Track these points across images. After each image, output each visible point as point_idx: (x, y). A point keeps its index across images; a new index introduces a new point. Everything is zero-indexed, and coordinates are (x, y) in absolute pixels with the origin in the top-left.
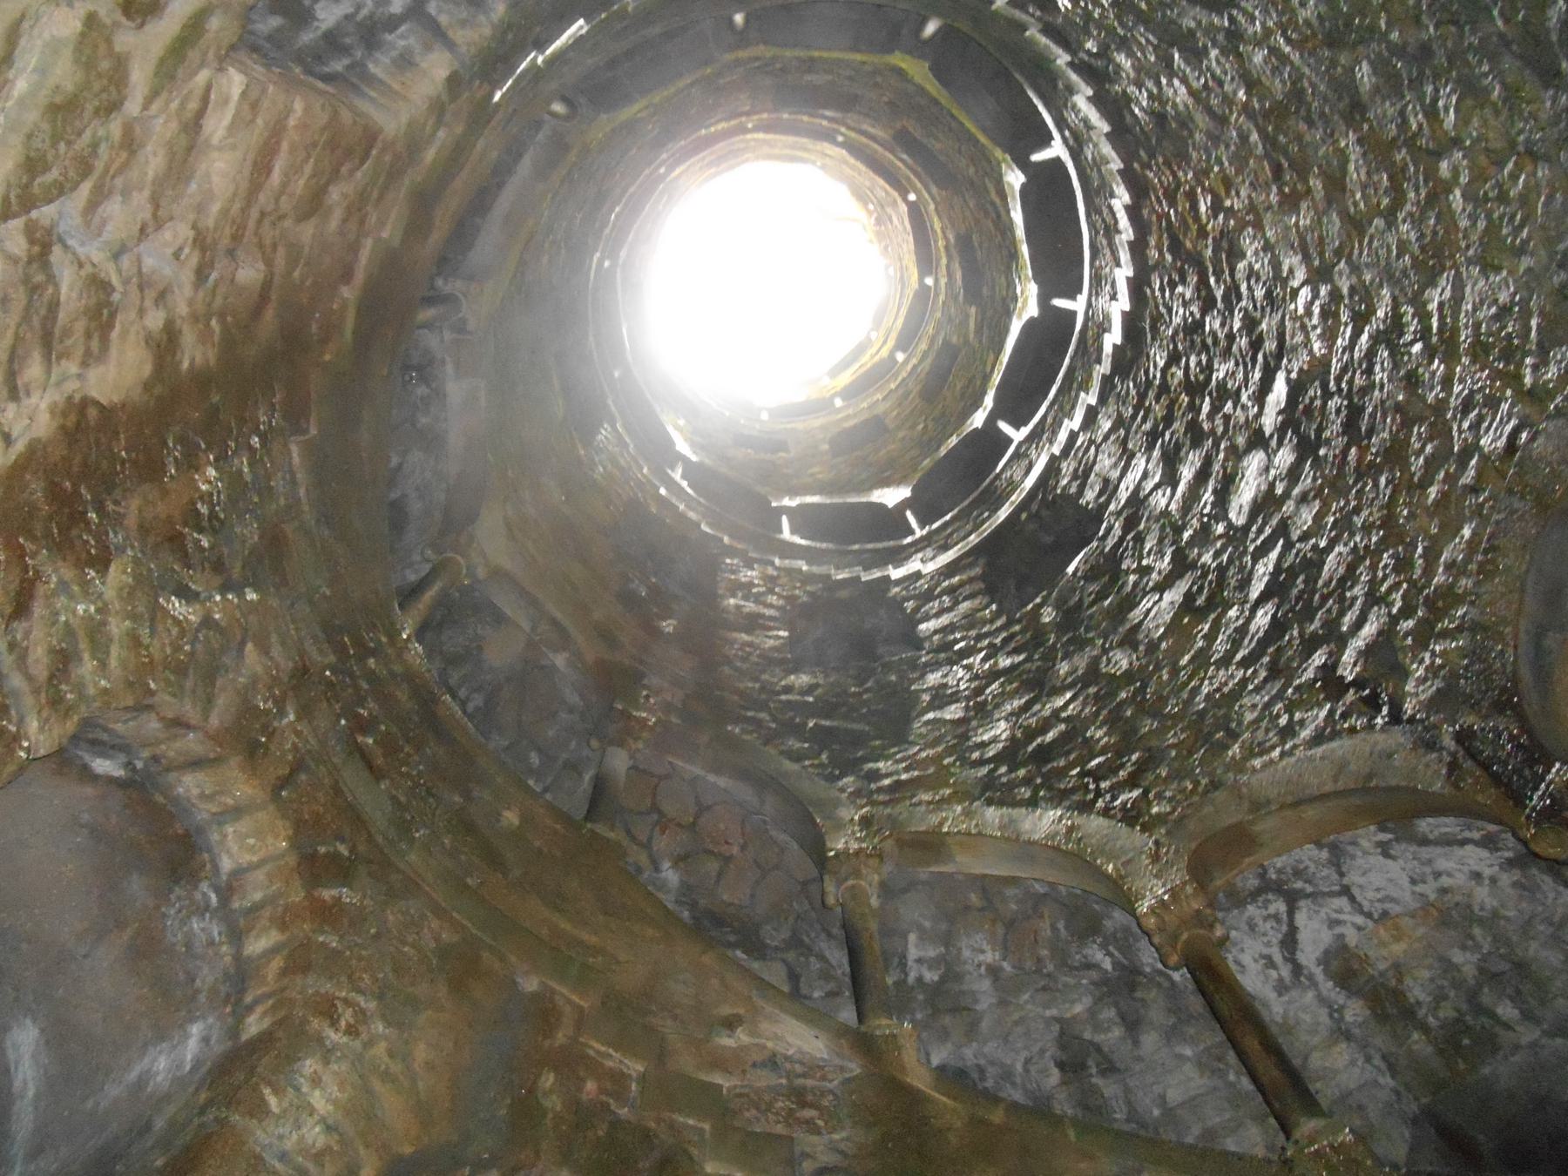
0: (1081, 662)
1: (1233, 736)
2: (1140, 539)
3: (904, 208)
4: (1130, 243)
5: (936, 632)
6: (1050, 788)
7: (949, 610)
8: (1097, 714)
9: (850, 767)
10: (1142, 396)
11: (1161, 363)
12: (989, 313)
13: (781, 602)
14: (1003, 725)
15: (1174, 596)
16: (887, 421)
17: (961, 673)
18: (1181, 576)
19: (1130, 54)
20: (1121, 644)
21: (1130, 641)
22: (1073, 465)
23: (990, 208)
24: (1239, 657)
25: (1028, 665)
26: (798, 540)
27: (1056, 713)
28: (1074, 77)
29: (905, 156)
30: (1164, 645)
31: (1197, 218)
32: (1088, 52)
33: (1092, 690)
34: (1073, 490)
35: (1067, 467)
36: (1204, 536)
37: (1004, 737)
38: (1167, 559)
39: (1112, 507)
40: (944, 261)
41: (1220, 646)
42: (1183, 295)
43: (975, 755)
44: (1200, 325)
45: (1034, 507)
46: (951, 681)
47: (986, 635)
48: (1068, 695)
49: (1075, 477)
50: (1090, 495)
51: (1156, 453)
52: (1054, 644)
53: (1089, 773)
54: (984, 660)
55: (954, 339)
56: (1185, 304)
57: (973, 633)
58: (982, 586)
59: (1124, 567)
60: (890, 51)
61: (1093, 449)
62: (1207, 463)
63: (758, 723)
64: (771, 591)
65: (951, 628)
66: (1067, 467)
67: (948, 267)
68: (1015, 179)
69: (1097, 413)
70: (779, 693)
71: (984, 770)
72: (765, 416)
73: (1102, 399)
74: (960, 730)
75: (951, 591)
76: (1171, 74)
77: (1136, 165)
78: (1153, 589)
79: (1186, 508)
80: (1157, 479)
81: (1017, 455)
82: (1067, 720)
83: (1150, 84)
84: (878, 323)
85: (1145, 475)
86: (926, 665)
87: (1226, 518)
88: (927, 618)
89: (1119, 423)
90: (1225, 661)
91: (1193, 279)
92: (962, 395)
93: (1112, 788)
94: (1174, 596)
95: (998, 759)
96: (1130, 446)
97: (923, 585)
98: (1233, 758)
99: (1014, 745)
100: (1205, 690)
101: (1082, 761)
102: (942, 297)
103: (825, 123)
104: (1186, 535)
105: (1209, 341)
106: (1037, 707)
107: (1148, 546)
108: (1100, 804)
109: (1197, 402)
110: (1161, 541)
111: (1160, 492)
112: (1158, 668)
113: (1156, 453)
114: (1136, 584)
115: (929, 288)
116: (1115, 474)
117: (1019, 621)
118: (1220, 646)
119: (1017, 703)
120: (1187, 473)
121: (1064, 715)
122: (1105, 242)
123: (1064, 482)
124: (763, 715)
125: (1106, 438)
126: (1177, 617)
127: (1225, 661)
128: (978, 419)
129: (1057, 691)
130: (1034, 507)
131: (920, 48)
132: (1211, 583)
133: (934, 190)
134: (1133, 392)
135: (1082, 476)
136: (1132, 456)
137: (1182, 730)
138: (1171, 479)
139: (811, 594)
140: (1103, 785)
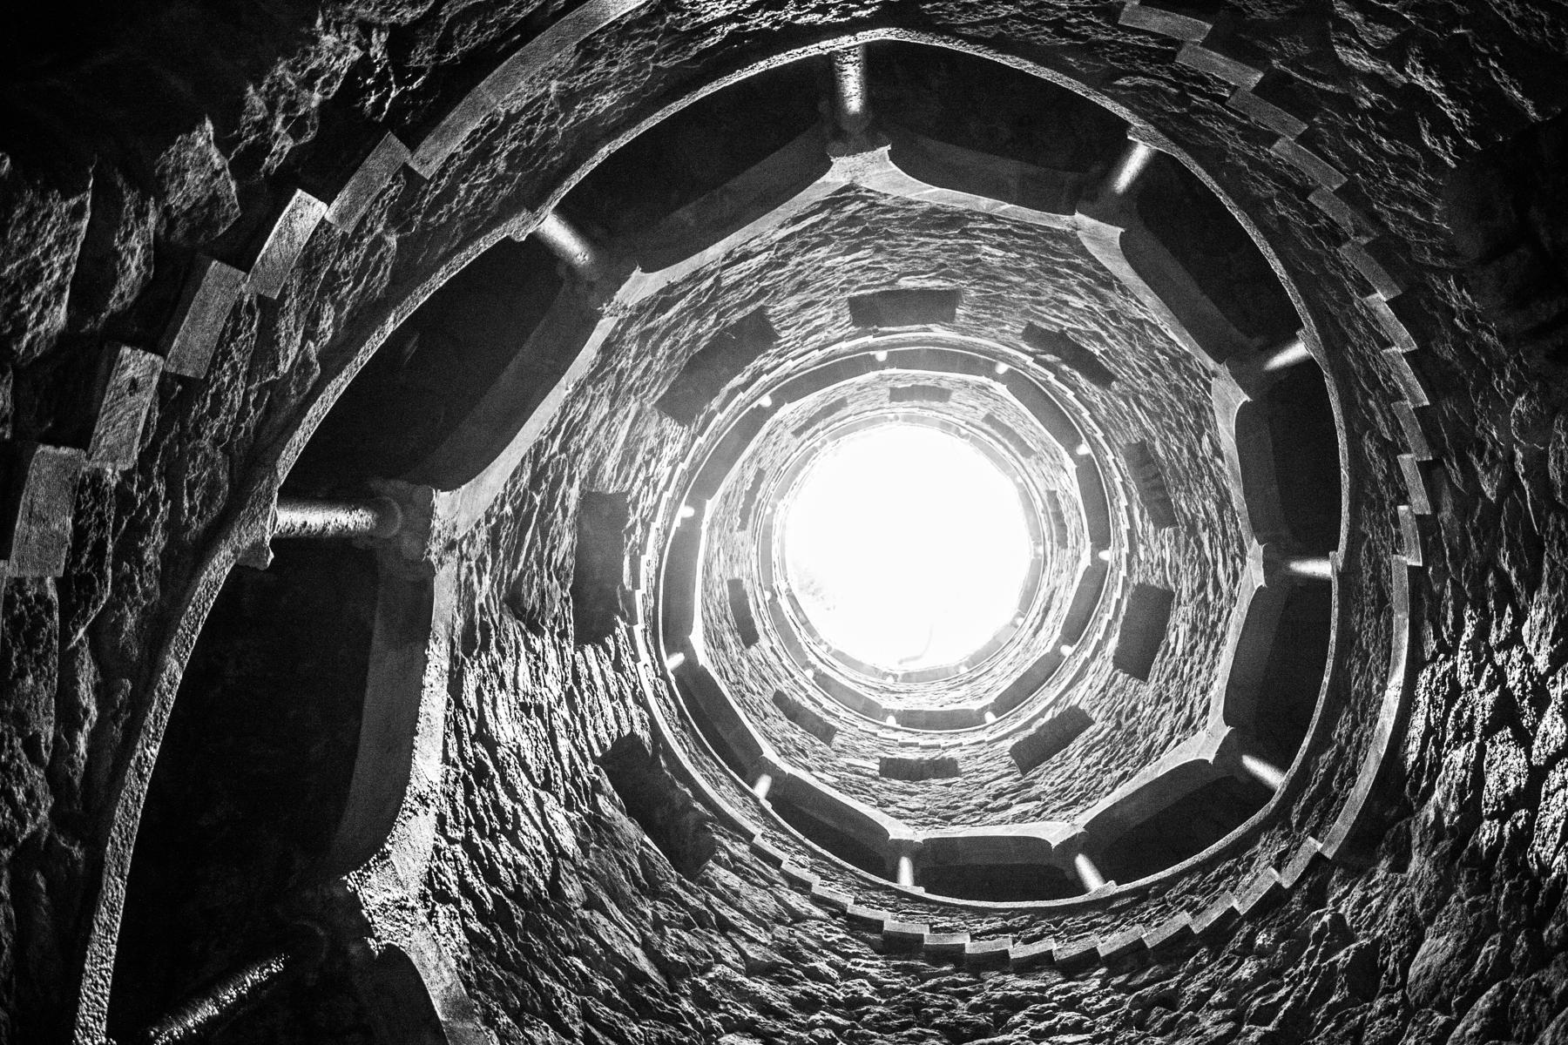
0: (567, 840)
1: (516, 1016)
2: (687, 926)
3: (976, 706)
4: (1006, 953)
5: (589, 668)
6: (456, 782)
7: (608, 690)
8: (522, 850)
9: (494, 541)
10: (829, 946)
11: (872, 972)
12: (876, 785)
13: (634, 493)
14: (511, 735)
15: (644, 964)
16: (753, 648)
17: (556, 693)
18: (661, 972)
19: (1258, 978)
20: (587, 889)
21: (592, 903)
22: (747, 858)
23: (1002, 801)
24: (594, 1031)
25: (559, 773)
26: (677, 523)
27: (521, 802)
28: (1214, 915)
29: (1048, 716)
30: (593, 942)
31: (1051, 1031)
32: (1252, 936)
33: (542, 848)
34: (722, 854)
35: (741, 850)
36: (704, 1000)
37: (501, 733)
38: (675, 957)
39: (714, 899)
40: (922, 742)
41: (603, 1011)
42: (954, 1007)
43: (487, 697)
44: (927, 1021)
45: (698, 805)
46: (549, 677)
47: (584, 727)
48: (537, 819)
49: (734, 858)
50: (721, 872)
51: (778, 958)
52: (579, 810)
53: (469, 836)
54: (566, 722)
55: (837, 739)
56: (946, 1007)
57: (587, 715)
58: (627, 731)
59: (659, 904)
60: (1228, 718)
61: (763, 882)
62: (780, 1015)
63: (553, 436)
64: (646, 481)
65: (592, 688)
66: (741, 850)
67: (916, 745)
68: (1055, 831)
69: (802, 893)
70: (571, 468)
71: (474, 705)
72: (769, 510)
73: (819, 901)
74: (508, 681)
75: (622, 698)
76: (1238, 1019)
77: (1103, 971)
78: (642, 935)
79: (726, 983)
80: (750, 953)
81: (744, 792)
82: (515, 810)
83: (1218, 996)
84: (839, 655)
85: (751, 940)
86: (562, 649)
87: (728, 1032)
88: (600, 660)
89: (798, 918)
90: (587, 1015)
91: (982, 1019)
92: (785, 740)
93: (456, 859)
94: (644, 964)
95: (482, 723)
96: (779, 928)
97: (626, 660)
98: (497, 1014)
99: (491, 745)
100: (560, 989)
101: (480, 826)
102: (881, 733)
103: (1099, 636)
104: (704, 982)
105: (915, 1030)
106: (526, 781)
107: (685, 935)
108: (444, 844)
109: (839, 1010)
110: (691, 951)
111: (738, 956)
112: (571, 933)
113: (778, 958)
114: (644, 915)
115: (884, 719)
116: (745, 905)
117: (596, 771)
118: (603, 1011)
119: (529, 755)
120: (763, 988)
121: (519, 808)
122: (998, 924)
123: (726, 842)
124: (555, 448)
125: (778, 899)
126: (617, 959)
127: (587, 1015)
128: (769, 753)
129: (540, 803)
130: (698, 805)
131: (1228, 750)
132: (662, 1006)
133: (1009, 743)
134: (834, 937)
135: (734, 865)
136: (767, 929)
137: (514, 954)
138: (754, 969)
139: (635, 524)
140: (458, 848)
